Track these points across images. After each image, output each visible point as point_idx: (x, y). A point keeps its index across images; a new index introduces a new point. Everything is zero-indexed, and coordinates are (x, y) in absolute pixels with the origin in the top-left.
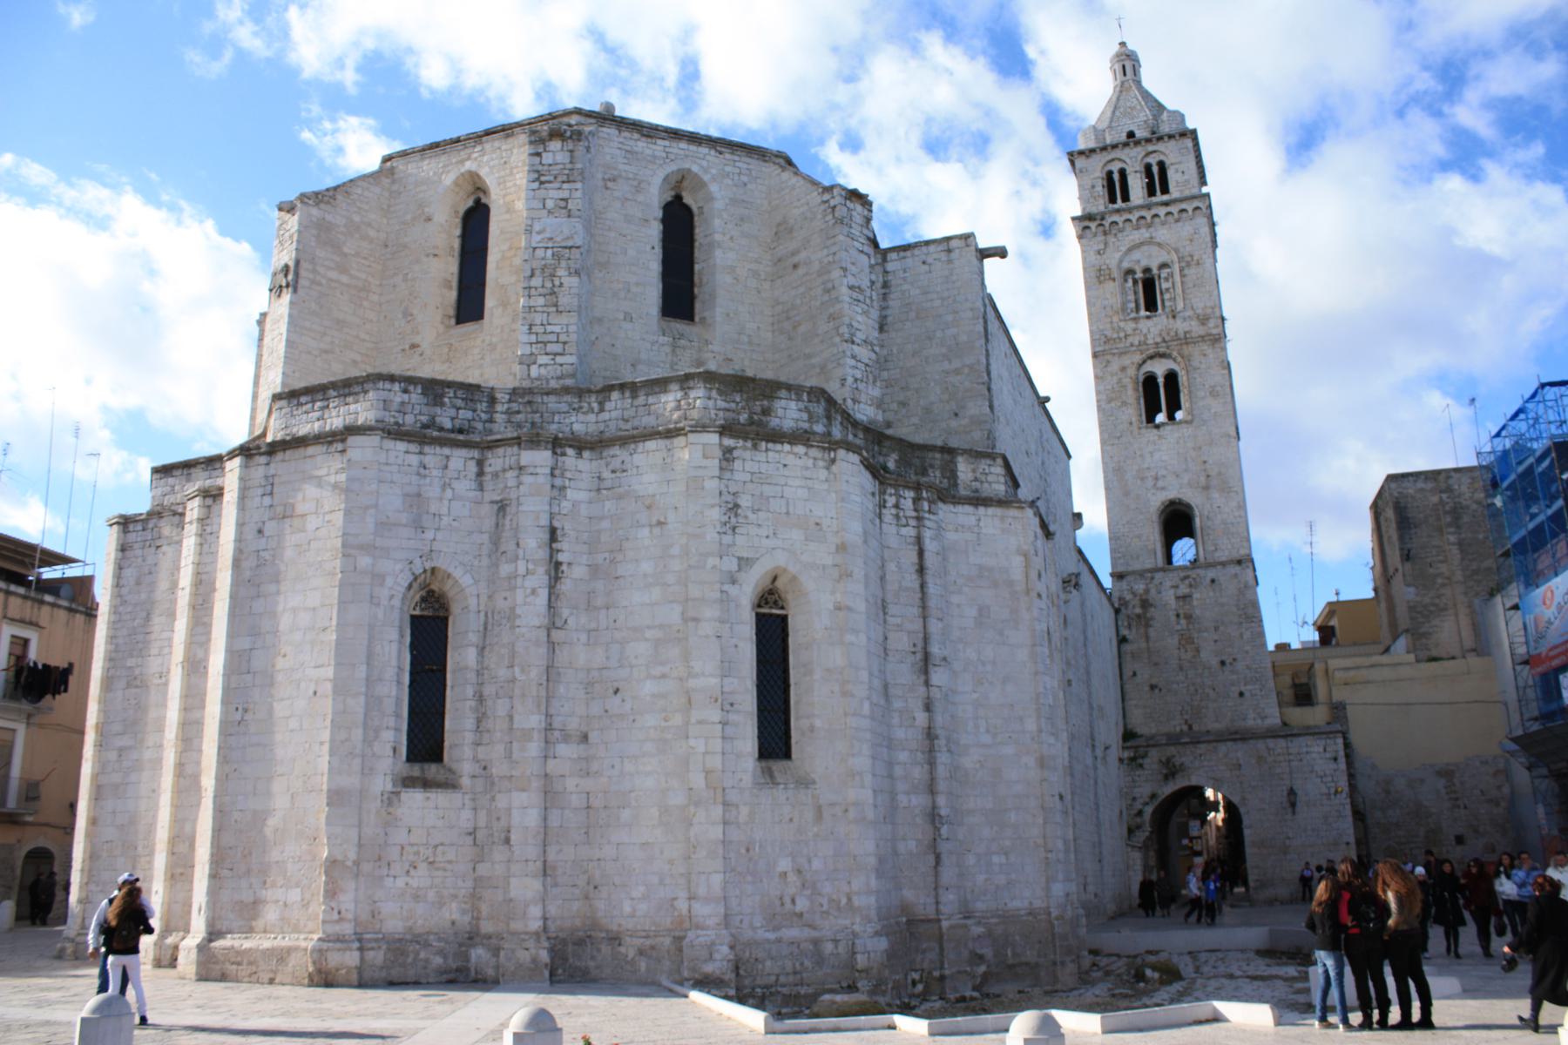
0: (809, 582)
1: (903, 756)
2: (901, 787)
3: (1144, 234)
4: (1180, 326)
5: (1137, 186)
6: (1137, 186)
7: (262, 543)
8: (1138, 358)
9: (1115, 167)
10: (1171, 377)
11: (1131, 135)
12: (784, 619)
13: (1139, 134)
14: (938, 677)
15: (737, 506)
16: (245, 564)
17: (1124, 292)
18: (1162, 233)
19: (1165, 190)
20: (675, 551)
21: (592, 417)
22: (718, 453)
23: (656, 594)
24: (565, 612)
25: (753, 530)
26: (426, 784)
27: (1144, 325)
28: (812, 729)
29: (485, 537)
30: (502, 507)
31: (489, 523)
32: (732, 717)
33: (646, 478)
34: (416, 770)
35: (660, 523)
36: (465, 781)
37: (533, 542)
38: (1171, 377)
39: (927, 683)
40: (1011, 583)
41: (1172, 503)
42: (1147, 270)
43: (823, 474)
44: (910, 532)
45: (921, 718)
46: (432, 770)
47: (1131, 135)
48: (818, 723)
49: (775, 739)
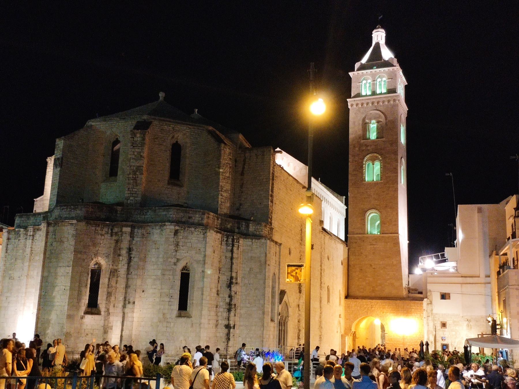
0: (195, 265)
1: (221, 310)
2: (220, 318)
7: (52, 248)
12: (189, 273)
14: (234, 288)
15: (178, 245)
16: (47, 253)
20: (161, 256)
21: (143, 217)
22: (174, 231)
23: (155, 266)
24: (132, 270)
25: (182, 251)
26: (92, 314)
28: (193, 303)
29: (112, 249)
30: (117, 241)
31: (113, 246)
32: (172, 300)
33: (155, 236)
34: (90, 310)
35: (158, 249)
36: (102, 313)
37: (124, 252)
39: (230, 290)
40: (260, 261)
43: (202, 236)
44: (230, 248)
45: (228, 300)
46: (94, 310)
48: (194, 302)
49: (183, 305)
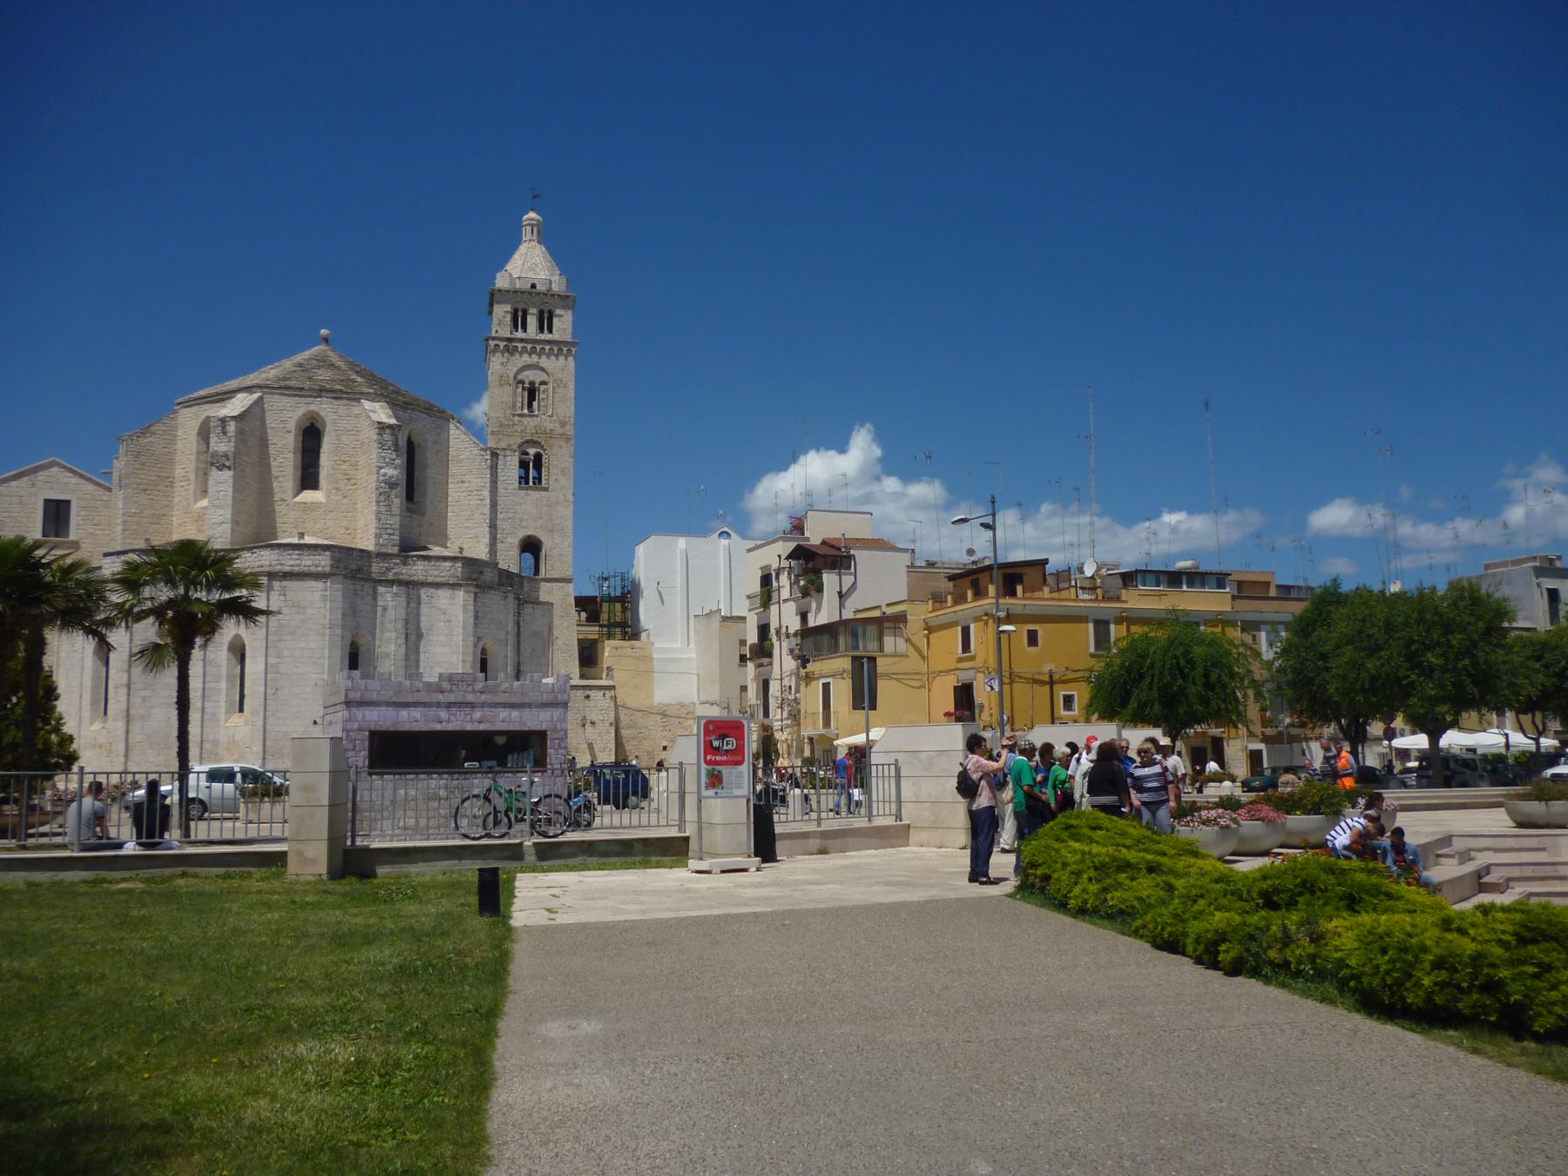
3: (535, 358)
4: (549, 425)
5: (532, 322)
6: (532, 322)
8: (519, 441)
9: (521, 306)
10: (538, 457)
11: (533, 286)
13: (539, 287)
17: (515, 395)
18: (544, 362)
19: (550, 331)
27: (526, 420)
38: (538, 457)
41: (529, 537)
42: (532, 383)
47: (533, 286)
